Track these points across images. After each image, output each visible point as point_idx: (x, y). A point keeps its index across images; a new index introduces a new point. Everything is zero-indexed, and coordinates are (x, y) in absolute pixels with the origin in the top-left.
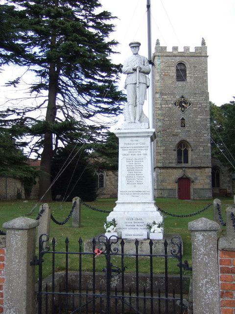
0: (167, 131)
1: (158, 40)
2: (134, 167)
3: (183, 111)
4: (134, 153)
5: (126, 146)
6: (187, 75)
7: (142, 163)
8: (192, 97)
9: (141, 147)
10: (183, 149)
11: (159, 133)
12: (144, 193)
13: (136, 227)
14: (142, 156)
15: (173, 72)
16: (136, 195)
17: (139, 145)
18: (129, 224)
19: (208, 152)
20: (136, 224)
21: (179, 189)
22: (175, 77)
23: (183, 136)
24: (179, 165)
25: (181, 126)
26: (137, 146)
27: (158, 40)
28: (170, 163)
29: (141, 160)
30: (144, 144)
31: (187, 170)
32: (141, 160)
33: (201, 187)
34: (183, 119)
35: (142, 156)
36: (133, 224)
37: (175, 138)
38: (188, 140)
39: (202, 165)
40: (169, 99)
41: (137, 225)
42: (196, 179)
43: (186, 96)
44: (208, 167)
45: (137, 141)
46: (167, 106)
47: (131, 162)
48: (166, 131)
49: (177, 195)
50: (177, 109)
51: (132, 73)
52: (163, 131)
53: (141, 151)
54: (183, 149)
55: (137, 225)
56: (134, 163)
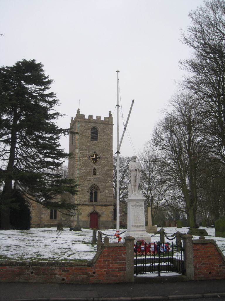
1: (78, 110)
6: (99, 137)
8: (101, 153)
11: (77, 179)
15: (89, 135)
21: (90, 221)
22: (90, 138)
23: (94, 182)
25: (93, 174)
27: (78, 110)
31: (96, 207)
33: (106, 219)
34: (95, 169)
38: (98, 185)
39: (107, 204)
40: (85, 153)
42: (103, 213)
43: (98, 153)
44: (111, 205)
46: (83, 158)
48: (82, 177)
49: (89, 225)
50: (90, 161)
52: (80, 177)
54: (94, 191)
56: (137, 213)
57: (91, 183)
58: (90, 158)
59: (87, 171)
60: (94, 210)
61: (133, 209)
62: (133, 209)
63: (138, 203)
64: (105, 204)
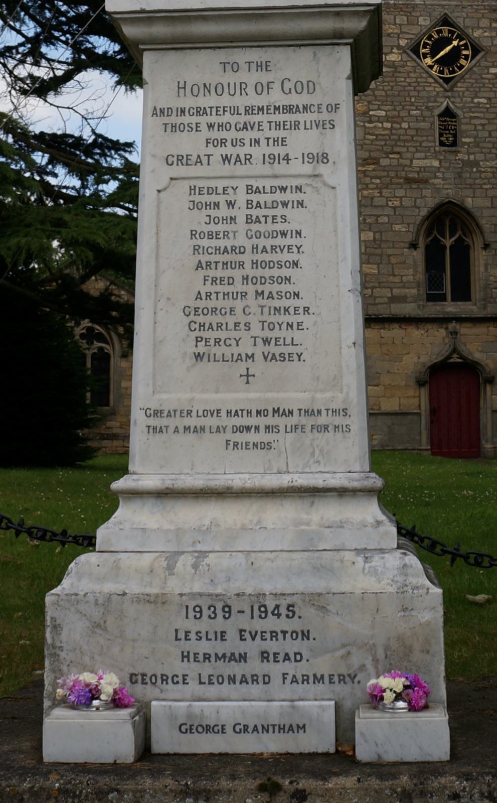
0: (384, 162)
3: (447, 81)
4: (242, 151)
5: (188, 102)
7: (296, 218)
9: (289, 109)
10: (448, 242)
12: (308, 421)
13: (255, 666)
14: (297, 167)
16: (252, 437)
17: (277, 97)
18: (204, 647)
20: (252, 648)
24: (434, 309)
25: (442, 144)
28: (393, 299)
29: (288, 196)
30: (311, 87)
31: (465, 330)
32: (288, 196)
34: (448, 113)
35: (297, 167)
36: (233, 645)
38: (469, 202)
41: (264, 656)
45: (264, 66)
47: (223, 212)
48: (376, 162)
54: (448, 242)
55: (264, 656)
56: (241, 219)
57: (427, 192)
59: (405, 125)
60: (455, 350)
61: (182, 160)
62: (182, 160)
63: (252, 78)
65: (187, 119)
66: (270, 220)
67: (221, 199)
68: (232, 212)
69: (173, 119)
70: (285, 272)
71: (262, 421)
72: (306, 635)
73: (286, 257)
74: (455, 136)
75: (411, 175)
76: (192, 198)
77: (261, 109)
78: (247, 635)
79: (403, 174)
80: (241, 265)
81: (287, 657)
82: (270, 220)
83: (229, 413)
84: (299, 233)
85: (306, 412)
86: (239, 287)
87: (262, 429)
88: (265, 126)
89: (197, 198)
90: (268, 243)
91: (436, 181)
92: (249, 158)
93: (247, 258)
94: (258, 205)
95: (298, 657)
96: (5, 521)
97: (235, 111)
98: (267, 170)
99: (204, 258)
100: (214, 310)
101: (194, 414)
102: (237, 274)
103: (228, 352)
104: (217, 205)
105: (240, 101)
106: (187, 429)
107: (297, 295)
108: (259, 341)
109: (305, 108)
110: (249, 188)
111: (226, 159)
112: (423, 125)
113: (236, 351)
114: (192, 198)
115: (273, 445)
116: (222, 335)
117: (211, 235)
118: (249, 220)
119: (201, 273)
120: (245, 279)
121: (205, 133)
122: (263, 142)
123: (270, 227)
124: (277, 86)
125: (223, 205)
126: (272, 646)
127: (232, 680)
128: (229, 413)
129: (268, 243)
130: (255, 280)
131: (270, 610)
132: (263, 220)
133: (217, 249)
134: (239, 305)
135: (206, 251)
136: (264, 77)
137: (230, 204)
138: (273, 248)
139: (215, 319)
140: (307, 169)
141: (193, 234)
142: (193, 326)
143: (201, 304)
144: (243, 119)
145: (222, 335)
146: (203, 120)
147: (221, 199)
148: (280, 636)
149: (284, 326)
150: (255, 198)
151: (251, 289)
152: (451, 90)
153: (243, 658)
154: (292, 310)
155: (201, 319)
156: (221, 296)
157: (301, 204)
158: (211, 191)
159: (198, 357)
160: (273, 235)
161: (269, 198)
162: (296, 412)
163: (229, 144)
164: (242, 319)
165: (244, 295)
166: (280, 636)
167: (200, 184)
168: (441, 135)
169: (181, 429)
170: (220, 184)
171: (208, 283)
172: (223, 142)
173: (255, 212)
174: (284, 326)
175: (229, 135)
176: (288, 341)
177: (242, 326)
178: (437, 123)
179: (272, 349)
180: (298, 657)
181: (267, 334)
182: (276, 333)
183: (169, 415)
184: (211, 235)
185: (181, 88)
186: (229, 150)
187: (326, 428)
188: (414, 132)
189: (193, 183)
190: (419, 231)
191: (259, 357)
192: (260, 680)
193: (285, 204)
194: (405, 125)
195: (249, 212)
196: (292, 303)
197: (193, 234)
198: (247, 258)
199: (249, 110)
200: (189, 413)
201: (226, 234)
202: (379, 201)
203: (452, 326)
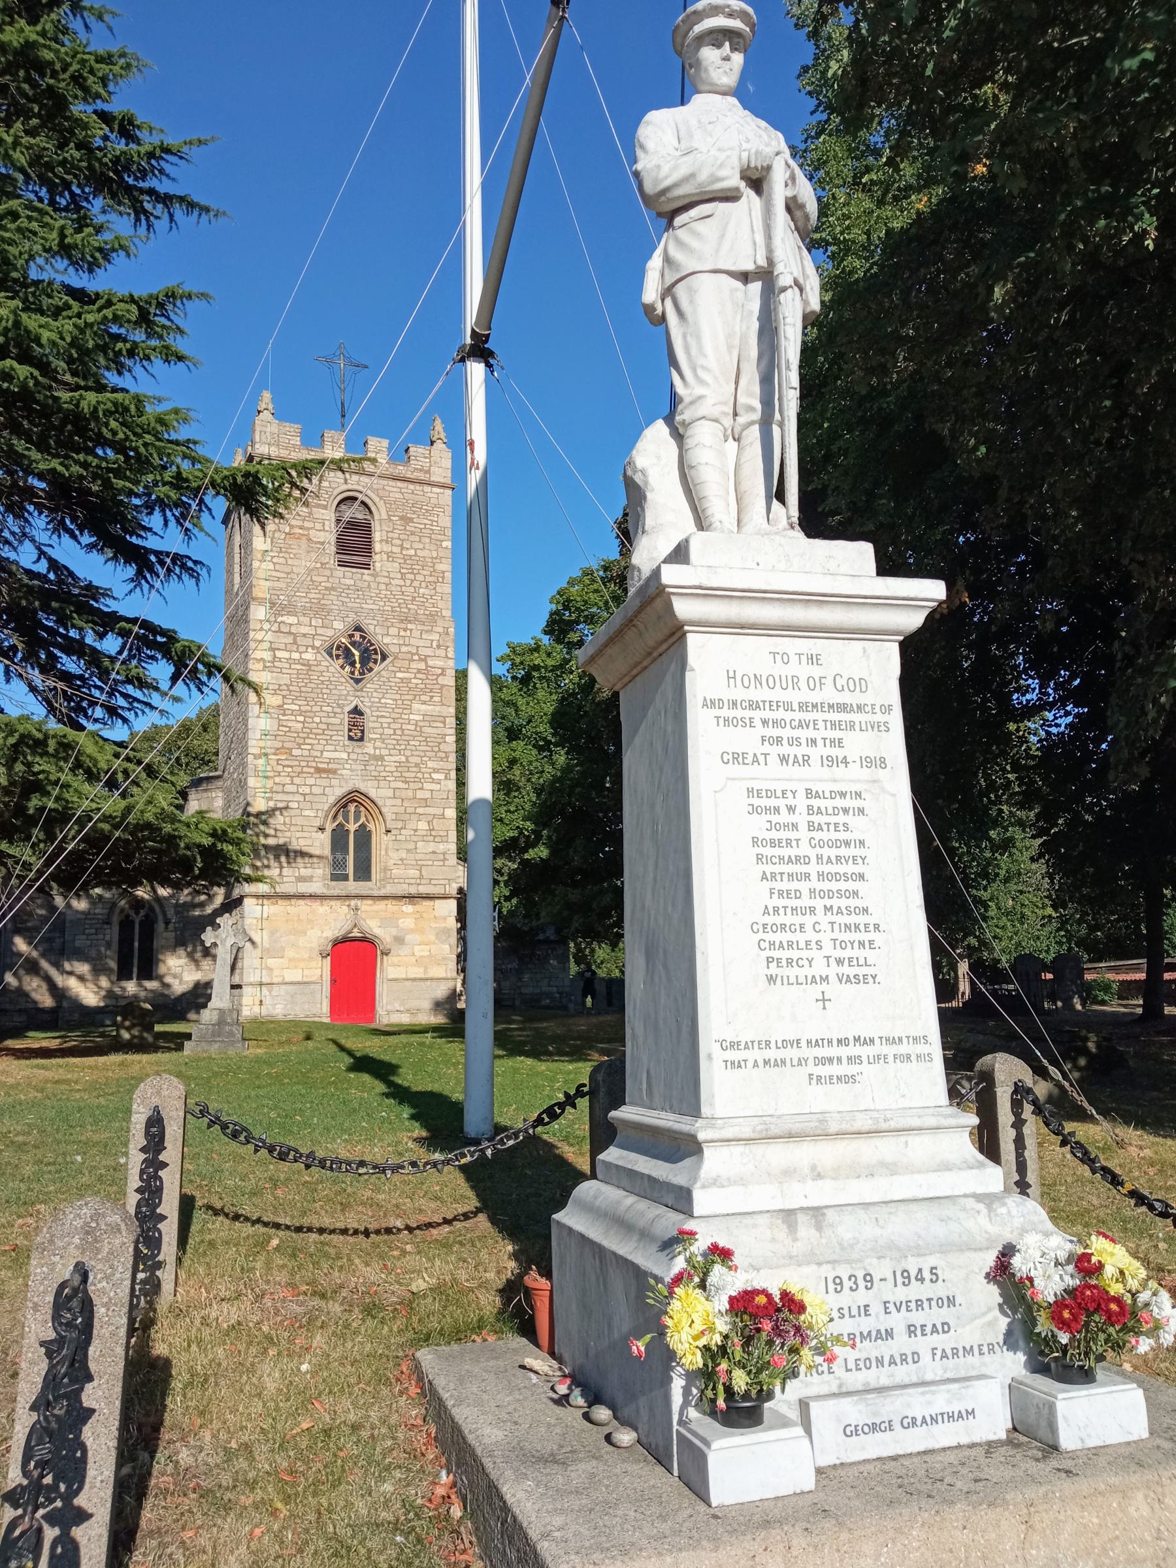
0: (296, 752)
2: (804, 850)
5: (739, 694)
8: (393, 631)
9: (843, 708)
10: (352, 827)
11: (262, 761)
16: (835, 1070)
17: (829, 695)
19: (444, 839)
20: (898, 1321)
26: (815, 697)
30: (860, 684)
31: (365, 906)
34: (356, 711)
37: (325, 782)
38: (372, 793)
39: (423, 890)
41: (911, 1330)
43: (371, 627)
44: (445, 897)
46: (296, 656)
47: (784, 817)
50: (334, 669)
51: (731, 196)
52: (277, 751)
53: (848, 737)
54: (352, 827)
56: (803, 827)
57: (334, 782)
58: (331, 655)
59: (317, 720)
60: (355, 926)
61: (738, 758)
62: (738, 758)
64: (413, 890)
65: (739, 713)
66: (832, 827)
67: (781, 803)
68: (792, 819)
69: (726, 712)
70: (851, 885)
71: (844, 1052)
72: (951, 1301)
73: (850, 868)
74: (363, 732)
75: (320, 765)
76: (751, 801)
77: (815, 706)
78: (892, 1308)
79: (314, 764)
80: (807, 876)
81: (935, 1330)
82: (832, 827)
83: (809, 1042)
84: (862, 843)
85: (887, 1040)
86: (806, 901)
87: (845, 1060)
88: (821, 725)
89: (756, 802)
90: (833, 853)
91: (344, 772)
92: (806, 760)
93: (813, 869)
94: (819, 812)
95: (946, 1327)
96: (292, 1153)
97: (788, 707)
98: (825, 772)
99: (769, 869)
100: (783, 927)
101: (773, 1045)
102: (804, 886)
103: (801, 973)
104: (777, 810)
105: (794, 697)
106: (766, 1062)
107: (866, 910)
108: (832, 961)
109: (859, 707)
110: (809, 793)
111: (784, 759)
112: (336, 721)
113: (809, 972)
114: (751, 801)
115: (858, 1078)
116: (794, 954)
117: (773, 843)
118: (811, 826)
119: (767, 885)
120: (812, 892)
121: (760, 731)
122: (820, 742)
123: (833, 835)
124: (829, 681)
125: (783, 810)
126: (918, 1318)
127: (880, 1362)
128: (809, 1042)
129: (833, 853)
130: (823, 894)
131: (913, 1274)
132: (825, 827)
133: (781, 858)
134: (808, 920)
135: (770, 860)
136: (816, 671)
137: (791, 809)
138: (839, 859)
139: (784, 937)
140: (865, 773)
141: (755, 841)
142: (763, 945)
143: (770, 919)
144: (798, 716)
145: (794, 954)
146: (758, 715)
147: (781, 803)
148: (926, 1305)
149: (856, 945)
150: (816, 803)
151: (819, 904)
152: (361, 690)
153: (889, 1334)
154: (862, 927)
155: (770, 937)
156: (789, 911)
157: (861, 811)
158: (770, 794)
159: (771, 979)
160: (836, 844)
161: (829, 804)
162: (877, 1041)
163: (785, 742)
164: (814, 937)
165: (812, 910)
166: (926, 1305)
167: (757, 785)
168: (350, 730)
169: (761, 1063)
170: (779, 787)
171: (775, 896)
172: (779, 740)
173: (816, 819)
174: (856, 945)
175: (786, 733)
176: (862, 962)
177: (813, 945)
178: (347, 719)
179: (846, 970)
180: (946, 1327)
181: (839, 953)
182: (848, 953)
183: (746, 1047)
184: (773, 843)
185: (731, 677)
186: (785, 749)
187: (909, 1057)
188: (324, 726)
189: (750, 784)
190: (327, 816)
191: (833, 978)
192: (910, 1359)
193: (846, 811)
194: (317, 720)
195: (811, 818)
196: (861, 919)
197: (755, 841)
198: (813, 869)
199: (803, 707)
200: (768, 1043)
201: (789, 843)
202: (289, 788)
203: (353, 903)
